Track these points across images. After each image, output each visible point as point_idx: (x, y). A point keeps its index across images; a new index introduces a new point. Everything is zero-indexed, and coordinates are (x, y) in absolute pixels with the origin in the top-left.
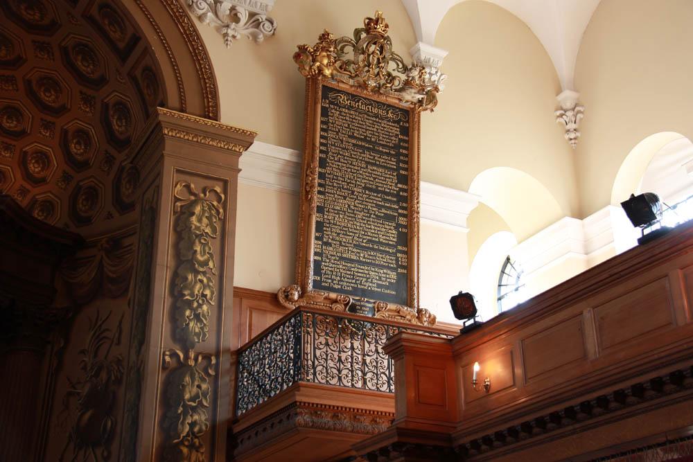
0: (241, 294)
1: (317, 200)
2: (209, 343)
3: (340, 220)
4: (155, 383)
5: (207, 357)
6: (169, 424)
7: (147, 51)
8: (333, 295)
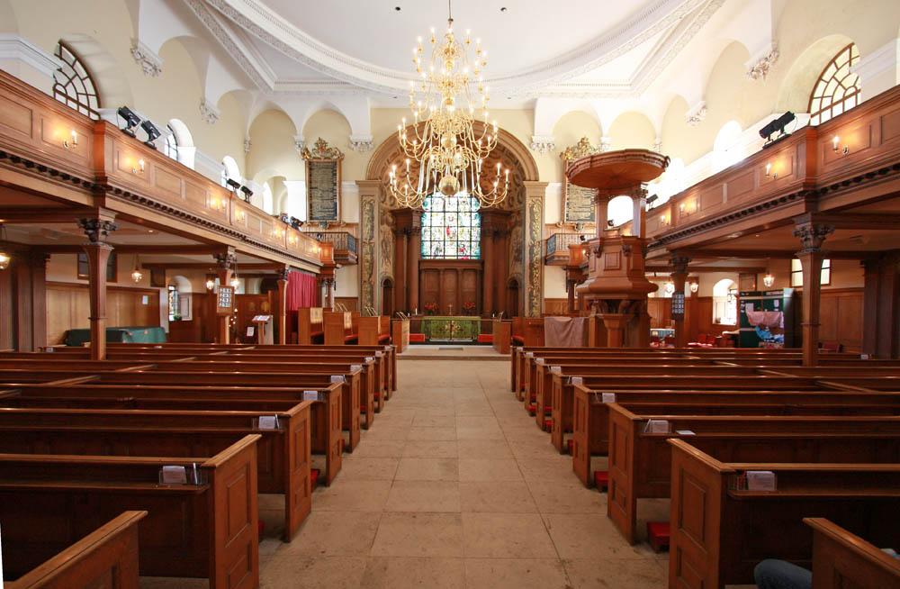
0: (546, 225)
1: (567, 197)
4: (527, 249)
7: (520, 164)
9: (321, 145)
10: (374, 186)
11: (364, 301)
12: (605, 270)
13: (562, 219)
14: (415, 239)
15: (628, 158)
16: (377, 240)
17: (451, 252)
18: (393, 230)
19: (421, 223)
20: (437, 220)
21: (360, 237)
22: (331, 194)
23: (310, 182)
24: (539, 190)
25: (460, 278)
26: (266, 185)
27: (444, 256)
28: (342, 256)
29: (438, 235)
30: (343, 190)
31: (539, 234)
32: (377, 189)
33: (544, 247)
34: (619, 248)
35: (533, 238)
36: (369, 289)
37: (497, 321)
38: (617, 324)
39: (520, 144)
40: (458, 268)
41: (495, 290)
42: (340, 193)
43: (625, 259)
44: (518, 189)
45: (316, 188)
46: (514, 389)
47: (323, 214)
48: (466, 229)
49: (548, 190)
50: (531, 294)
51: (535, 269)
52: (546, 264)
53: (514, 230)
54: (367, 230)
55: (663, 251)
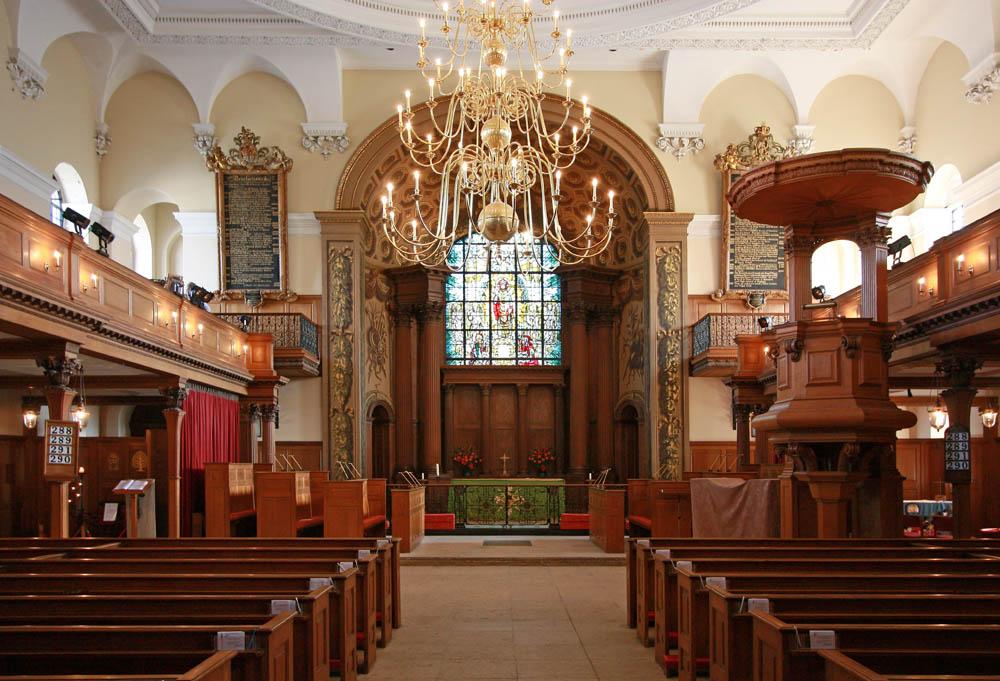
0: (692, 297)
1: (730, 241)
2: (678, 325)
3: (745, 250)
5: (677, 332)
6: (662, 364)
8: (740, 291)
9: (247, 141)
10: (352, 221)
11: (335, 449)
12: (808, 385)
13: (721, 284)
14: (433, 326)
15: (847, 166)
16: (357, 328)
17: (504, 351)
18: (388, 309)
19: (445, 296)
20: (476, 289)
21: (324, 323)
22: (267, 239)
23: (226, 214)
24: (678, 230)
25: (523, 401)
26: (140, 221)
27: (491, 359)
28: (291, 360)
29: (480, 318)
30: (291, 231)
31: (677, 315)
32: (357, 228)
33: (687, 342)
34: (837, 342)
35: (664, 324)
36: (344, 426)
37: (597, 490)
38: (835, 492)
39: (636, 140)
40: (519, 384)
41: (592, 425)
42: (285, 236)
43: (847, 363)
44: (634, 227)
45: (235, 226)
46: (633, 623)
47: (253, 278)
48: (533, 307)
49: (691, 228)
50: (663, 433)
51: (671, 384)
52: (691, 375)
53: (628, 307)
54: (337, 309)
55: (924, 347)
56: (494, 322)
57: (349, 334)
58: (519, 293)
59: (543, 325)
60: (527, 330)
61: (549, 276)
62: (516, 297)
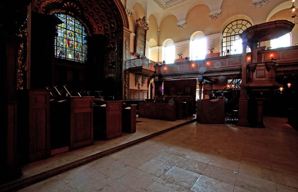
6: (125, 68)
17: (70, 56)
56: (67, 46)
57: (26, 33)
58: (76, 39)
59: (82, 51)
60: (78, 51)
61: (84, 37)
62: (75, 40)
